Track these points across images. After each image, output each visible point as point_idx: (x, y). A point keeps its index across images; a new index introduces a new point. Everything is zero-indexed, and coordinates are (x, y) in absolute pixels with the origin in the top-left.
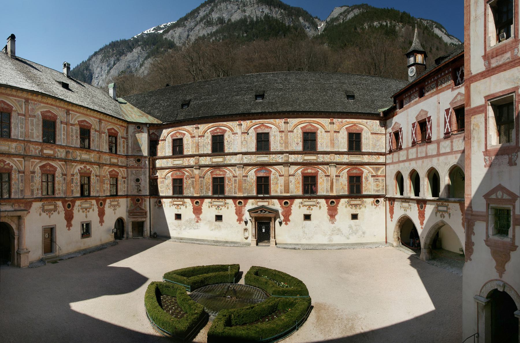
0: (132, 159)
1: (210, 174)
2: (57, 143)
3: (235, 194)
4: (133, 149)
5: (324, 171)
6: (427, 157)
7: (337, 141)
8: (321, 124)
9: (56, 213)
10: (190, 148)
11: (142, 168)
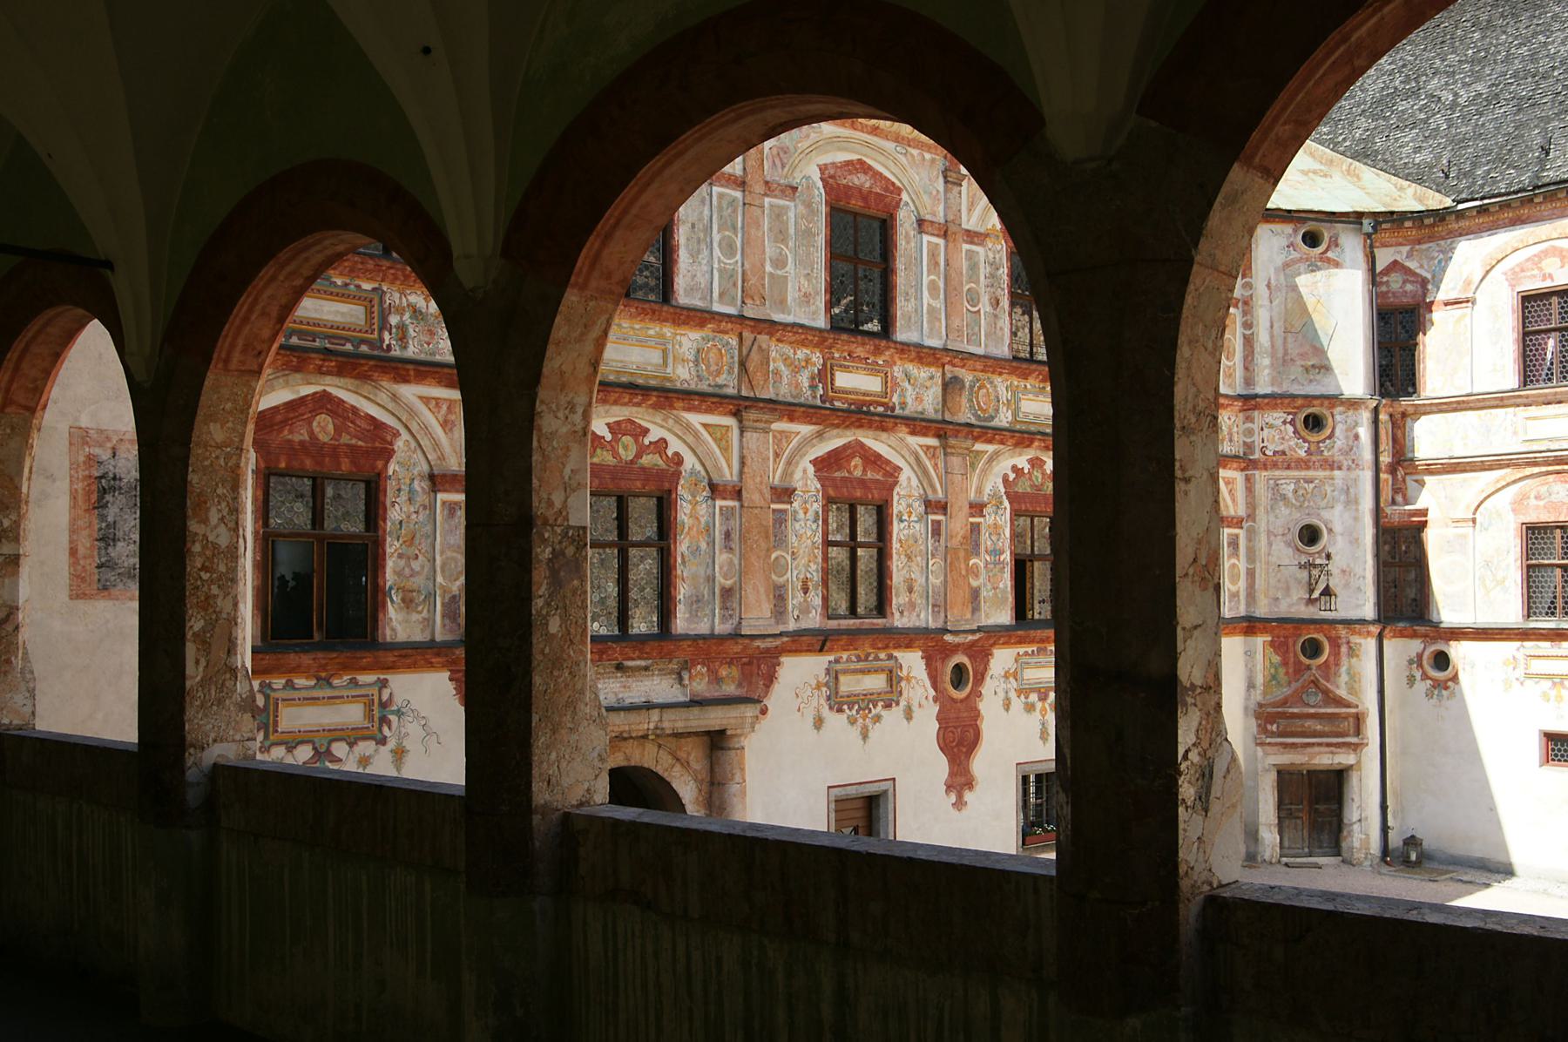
0: (1276, 417)
2: (902, 334)
4: (1283, 362)
9: (897, 712)
11: (1331, 465)
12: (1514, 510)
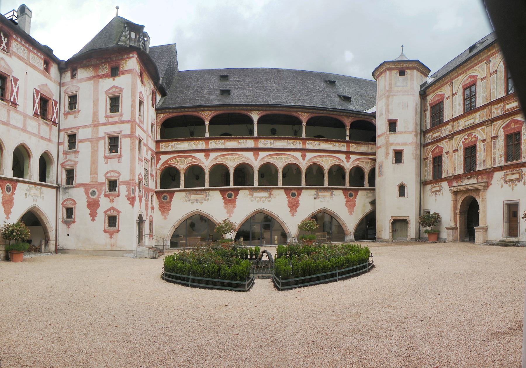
9: (521, 183)
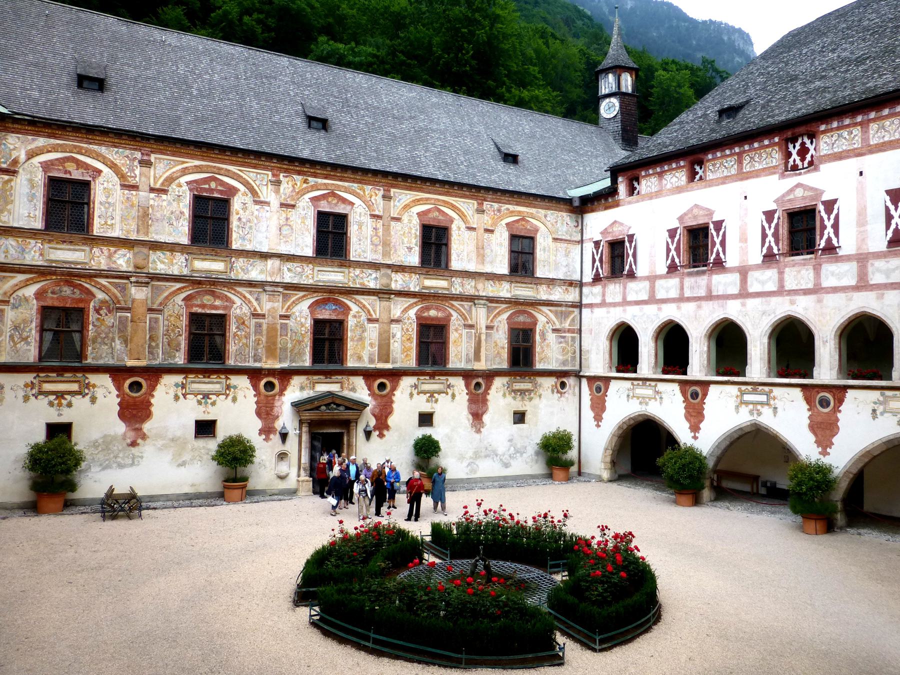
1: (180, 303)
3: (255, 361)
5: (464, 314)
6: (710, 297)
7: (489, 251)
8: (459, 210)
10: (118, 218)
12: (36, 298)
